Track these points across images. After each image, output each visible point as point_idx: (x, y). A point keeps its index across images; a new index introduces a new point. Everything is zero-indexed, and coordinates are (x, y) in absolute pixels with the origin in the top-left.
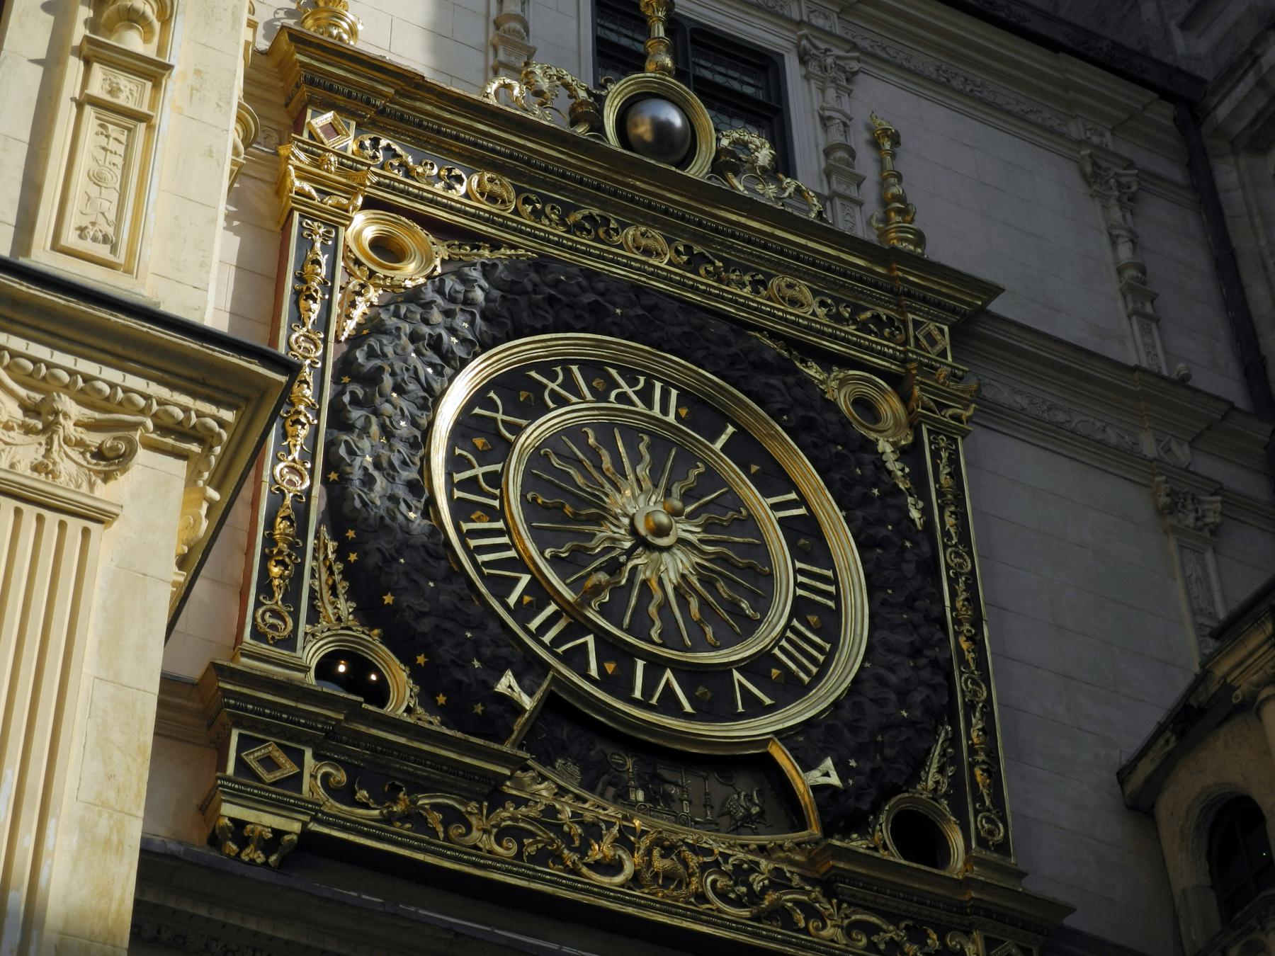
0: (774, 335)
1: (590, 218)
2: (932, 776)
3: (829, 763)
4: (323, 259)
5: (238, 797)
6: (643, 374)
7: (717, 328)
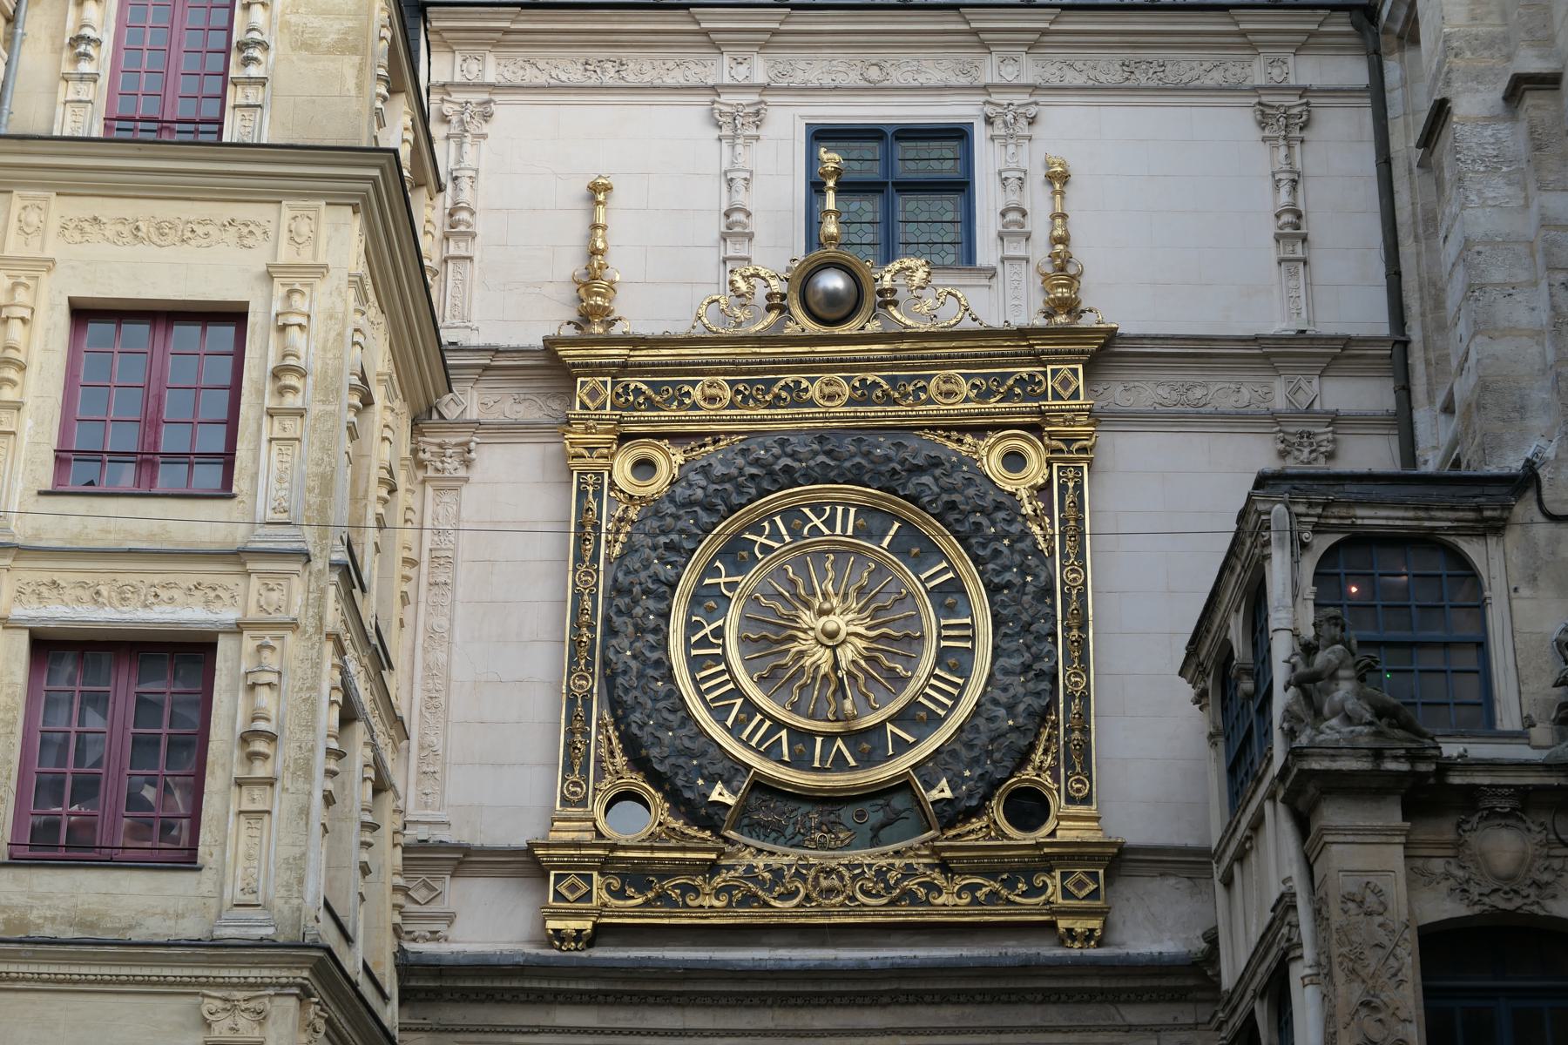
0: (933, 428)
1: (786, 387)
2: (1037, 757)
3: (944, 781)
4: (594, 506)
5: (557, 915)
6: (827, 504)
7: (883, 447)
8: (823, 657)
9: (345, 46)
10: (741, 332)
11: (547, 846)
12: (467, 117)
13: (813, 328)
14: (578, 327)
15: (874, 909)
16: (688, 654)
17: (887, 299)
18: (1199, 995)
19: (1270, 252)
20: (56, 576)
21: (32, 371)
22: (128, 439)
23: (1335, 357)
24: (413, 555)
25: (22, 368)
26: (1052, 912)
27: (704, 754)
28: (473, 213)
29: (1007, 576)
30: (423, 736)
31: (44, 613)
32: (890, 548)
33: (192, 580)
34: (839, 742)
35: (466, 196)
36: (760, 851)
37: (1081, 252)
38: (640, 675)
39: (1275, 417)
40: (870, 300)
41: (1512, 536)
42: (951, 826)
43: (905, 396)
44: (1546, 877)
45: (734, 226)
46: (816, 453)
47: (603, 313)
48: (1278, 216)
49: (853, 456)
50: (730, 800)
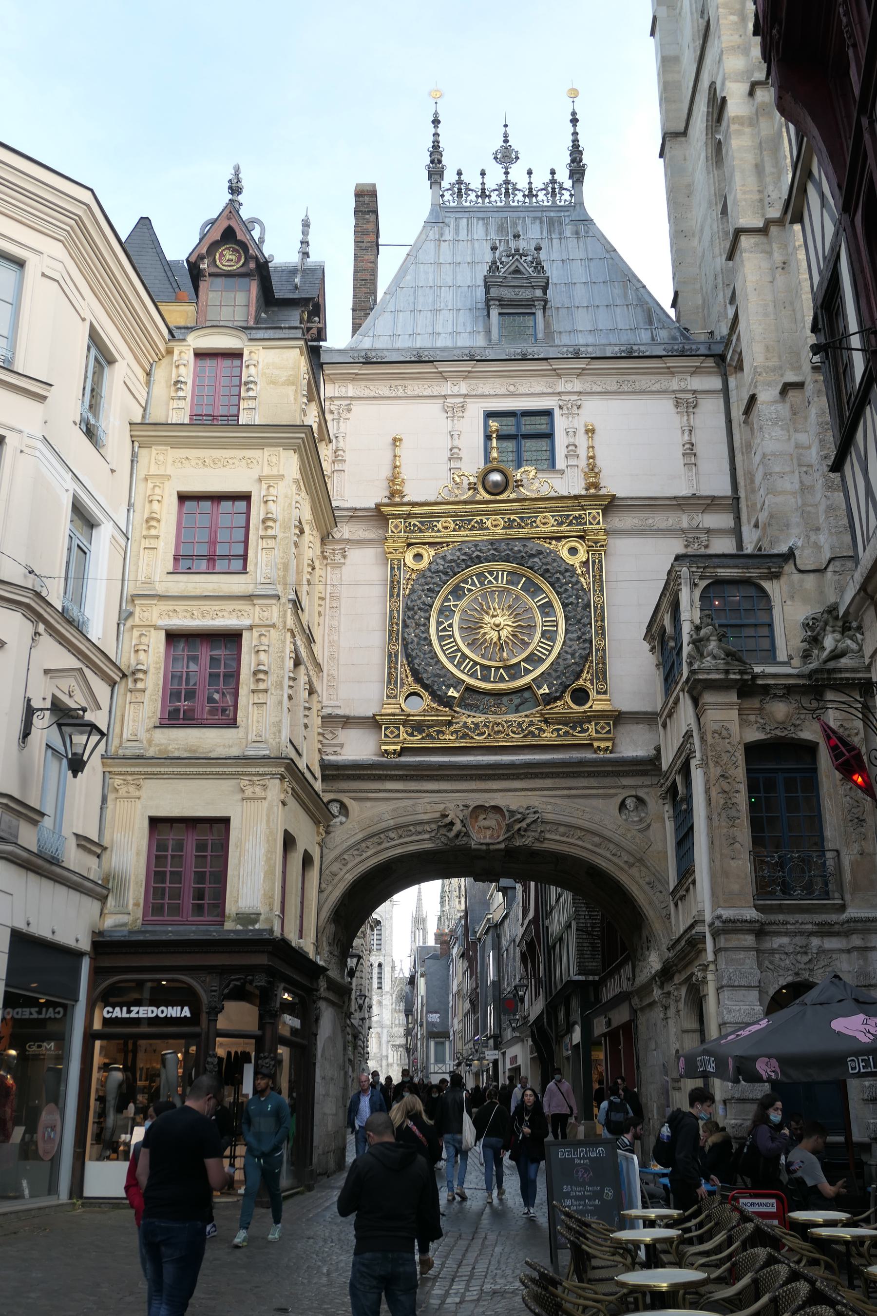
0: (539, 538)
2: (584, 675)
4: (397, 573)
5: (385, 744)
8: (494, 635)
9: (290, 382)
10: (457, 499)
11: (381, 715)
12: (341, 411)
13: (488, 497)
14: (389, 498)
15: (517, 739)
16: (438, 635)
17: (519, 484)
18: (653, 773)
19: (681, 461)
20: (175, 608)
21: (163, 522)
22: (204, 550)
23: (708, 505)
24: (323, 595)
25: (159, 521)
26: (591, 739)
27: (445, 676)
28: (344, 452)
29: (571, 600)
30: (329, 670)
31: (171, 623)
32: (522, 589)
33: (231, 608)
34: (501, 670)
35: (341, 445)
36: (469, 716)
37: (600, 462)
38: (418, 644)
39: (683, 531)
40: (512, 484)
41: (784, 579)
42: (549, 704)
43: (527, 525)
44: (798, 722)
45: (454, 455)
46: (490, 550)
47: (400, 493)
48: (684, 446)
49: (505, 550)
50: (456, 695)
